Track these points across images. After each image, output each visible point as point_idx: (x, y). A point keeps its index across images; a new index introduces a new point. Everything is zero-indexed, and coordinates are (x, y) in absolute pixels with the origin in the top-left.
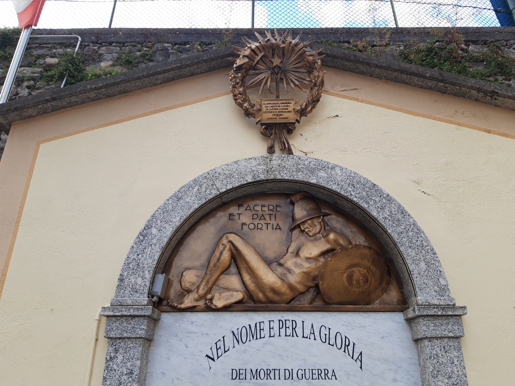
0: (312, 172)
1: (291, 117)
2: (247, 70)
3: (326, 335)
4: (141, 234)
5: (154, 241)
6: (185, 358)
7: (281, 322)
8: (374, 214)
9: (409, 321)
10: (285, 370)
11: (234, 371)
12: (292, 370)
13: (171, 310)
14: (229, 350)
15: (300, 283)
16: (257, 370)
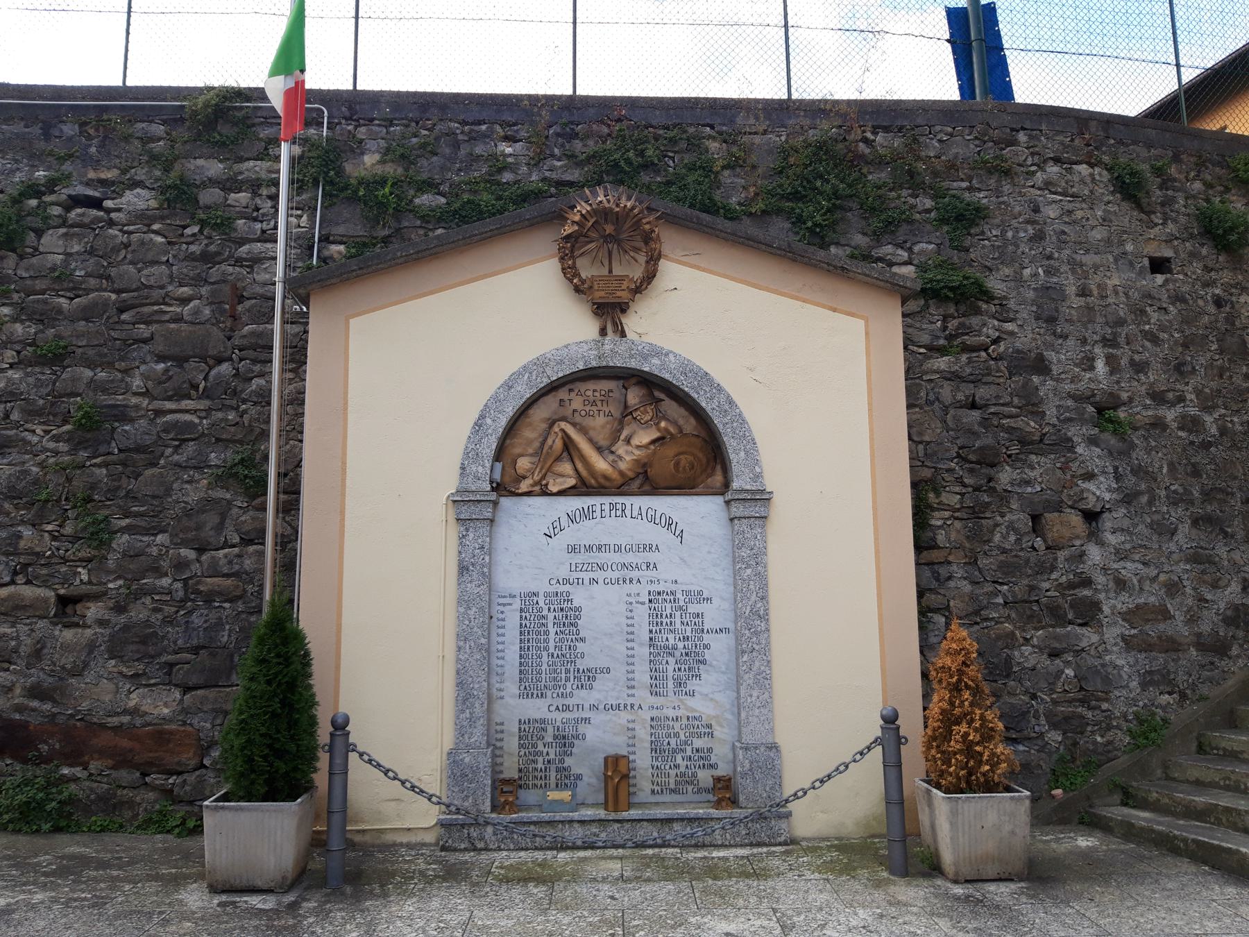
0: (645, 357)
1: (624, 295)
2: (577, 239)
4: (476, 424)
5: (490, 431)
8: (703, 404)
9: (728, 503)
15: (630, 470)
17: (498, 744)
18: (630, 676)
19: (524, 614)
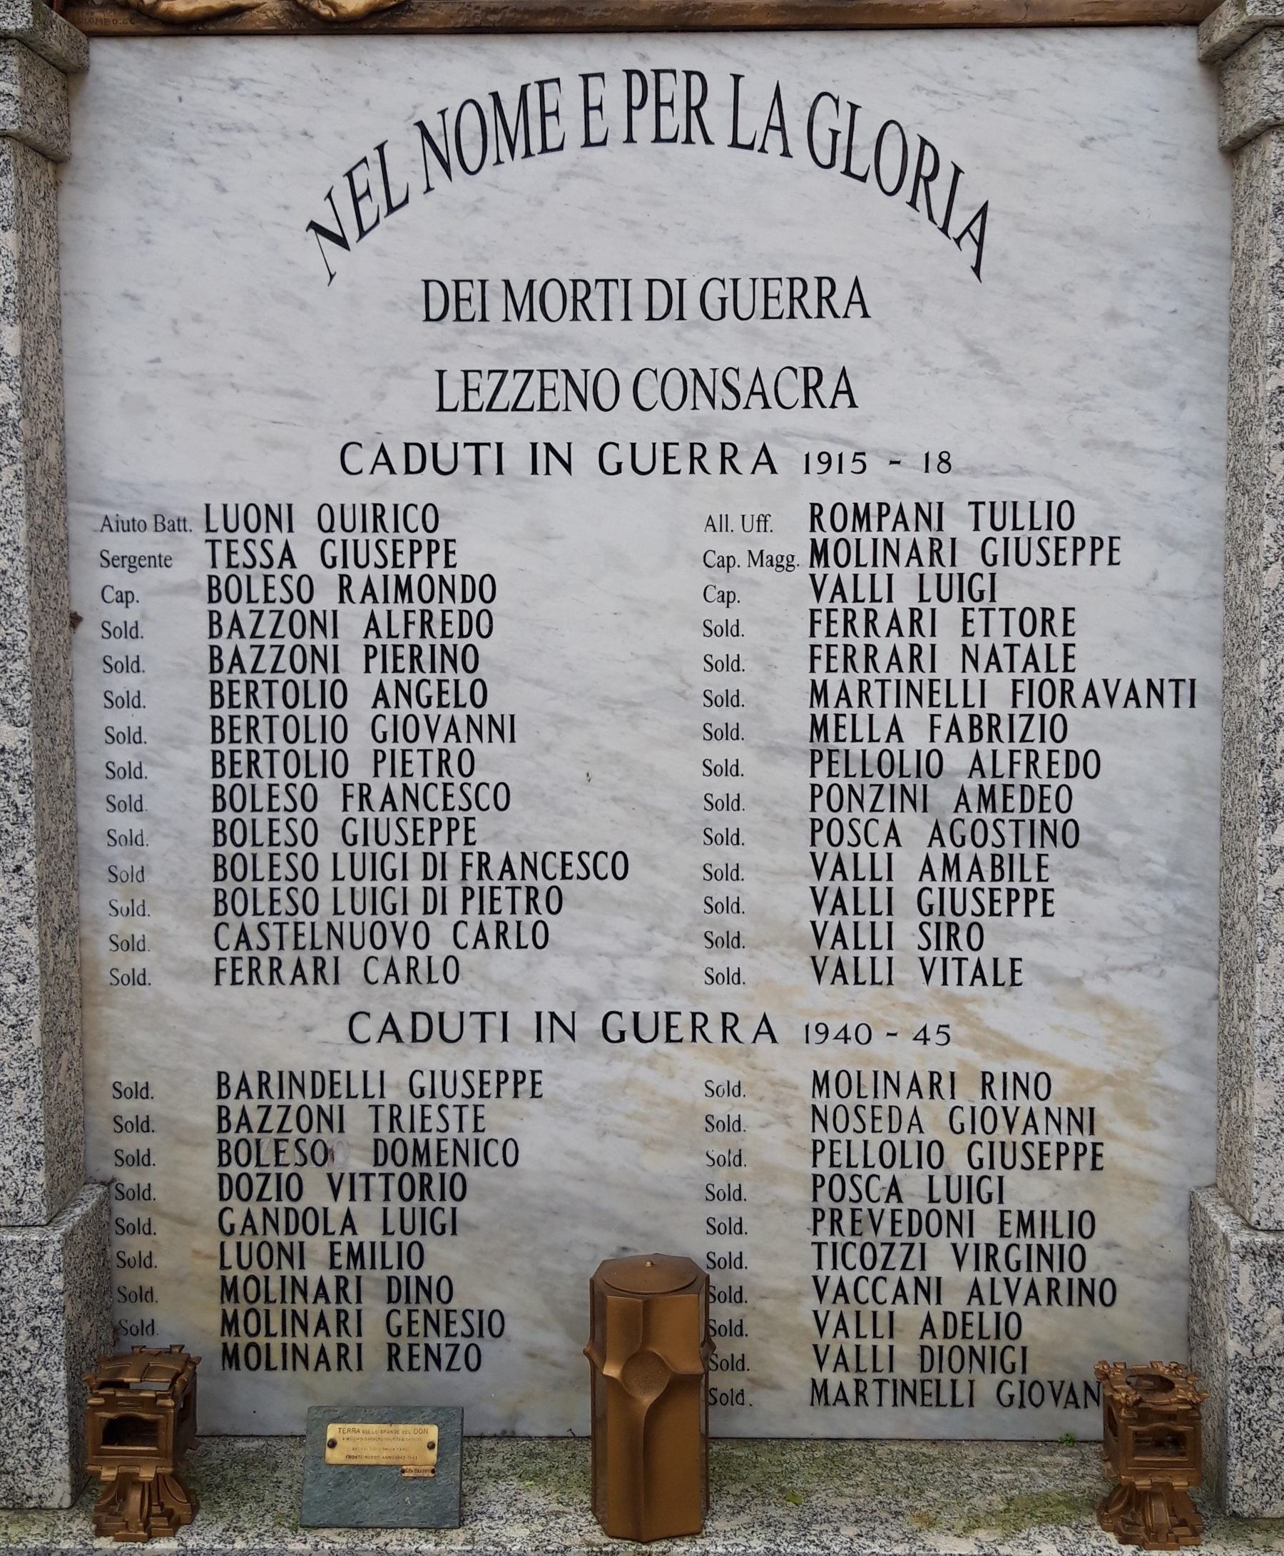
3: (835, 133)
6: (217, 234)
7: (635, 78)
10: (651, 281)
11: (435, 290)
12: (681, 281)
13: (129, 27)
14: (406, 201)
16: (531, 283)
17: (129, 1177)
18: (722, 890)
19: (226, 610)
